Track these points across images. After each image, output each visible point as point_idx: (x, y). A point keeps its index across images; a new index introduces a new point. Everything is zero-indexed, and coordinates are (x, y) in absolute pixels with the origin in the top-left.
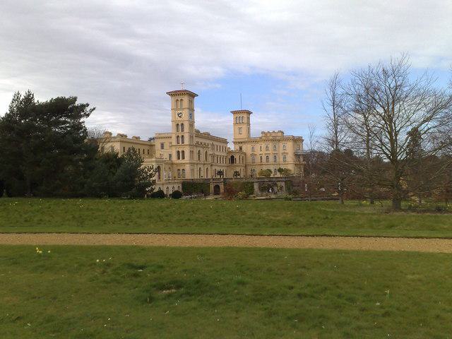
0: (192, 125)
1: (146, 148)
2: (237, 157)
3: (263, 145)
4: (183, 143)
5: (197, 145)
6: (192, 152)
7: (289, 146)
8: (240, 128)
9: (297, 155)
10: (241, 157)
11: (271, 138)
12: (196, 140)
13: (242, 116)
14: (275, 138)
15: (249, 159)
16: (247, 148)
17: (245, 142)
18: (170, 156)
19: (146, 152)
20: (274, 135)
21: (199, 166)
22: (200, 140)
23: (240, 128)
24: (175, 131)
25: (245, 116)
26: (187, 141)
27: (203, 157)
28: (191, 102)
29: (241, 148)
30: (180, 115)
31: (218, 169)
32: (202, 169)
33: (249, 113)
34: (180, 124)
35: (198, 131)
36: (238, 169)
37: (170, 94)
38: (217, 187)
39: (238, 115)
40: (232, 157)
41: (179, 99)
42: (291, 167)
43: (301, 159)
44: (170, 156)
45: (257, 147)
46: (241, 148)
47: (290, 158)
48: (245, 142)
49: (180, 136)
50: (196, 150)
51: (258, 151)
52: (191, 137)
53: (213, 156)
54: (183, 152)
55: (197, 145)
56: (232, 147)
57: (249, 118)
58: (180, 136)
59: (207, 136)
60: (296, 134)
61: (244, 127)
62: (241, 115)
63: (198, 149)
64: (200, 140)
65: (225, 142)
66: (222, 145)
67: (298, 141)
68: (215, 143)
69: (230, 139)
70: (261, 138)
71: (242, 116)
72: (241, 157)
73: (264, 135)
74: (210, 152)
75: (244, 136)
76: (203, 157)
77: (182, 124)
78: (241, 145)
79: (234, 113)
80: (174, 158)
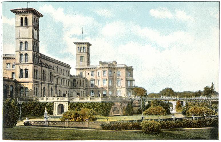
6: (35, 71)
13: (84, 48)
29: (81, 73)
33: (89, 45)
34: (24, 41)
37: (11, 10)
39: (80, 46)
40: (74, 80)
46: (81, 73)
56: (74, 72)
57: (88, 49)
58: (24, 53)
60: (129, 64)
61: (85, 56)
62: (83, 46)
65: (69, 67)
66: (66, 69)
68: (59, 66)
71: (84, 48)
77: (26, 42)
78: (82, 71)
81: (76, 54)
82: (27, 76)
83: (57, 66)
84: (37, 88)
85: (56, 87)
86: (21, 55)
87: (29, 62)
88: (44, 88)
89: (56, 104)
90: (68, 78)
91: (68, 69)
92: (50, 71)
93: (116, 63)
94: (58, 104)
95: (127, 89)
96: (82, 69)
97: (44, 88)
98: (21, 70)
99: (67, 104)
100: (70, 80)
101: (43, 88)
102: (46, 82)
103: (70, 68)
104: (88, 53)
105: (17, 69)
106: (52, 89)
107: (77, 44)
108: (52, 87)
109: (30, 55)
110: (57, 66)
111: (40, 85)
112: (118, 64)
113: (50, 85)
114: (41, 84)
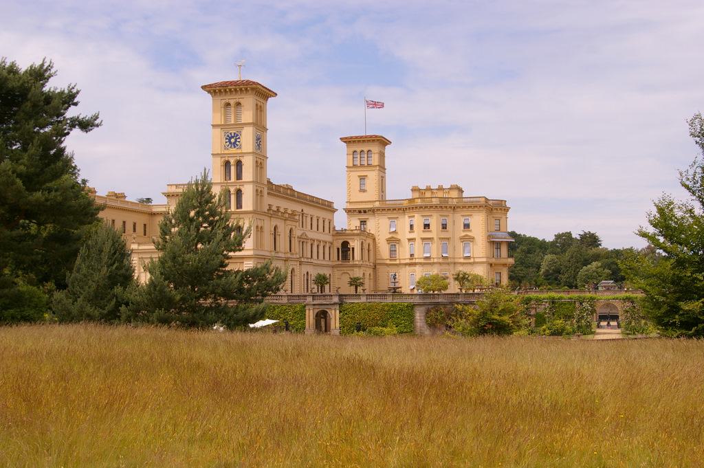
0: (260, 165)
1: (141, 220)
2: (355, 244)
3: (418, 220)
5: (272, 213)
6: (260, 229)
8: (362, 178)
9: (495, 244)
10: (366, 246)
11: (435, 202)
12: (268, 200)
14: (443, 204)
15: (384, 250)
16: (379, 227)
17: (373, 211)
19: (140, 229)
20: (440, 194)
23: (362, 178)
25: (375, 149)
27: (283, 244)
28: (260, 110)
29: (363, 222)
30: (233, 140)
31: (314, 272)
33: (383, 142)
34: (232, 161)
35: (269, 182)
36: (357, 273)
37: (204, 87)
38: (322, 316)
40: (345, 244)
41: (232, 102)
42: (480, 271)
43: (504, 250)
45: (404, 222)
46: (363, 222)
47: (480, 250)
48: (373, 211)
49: (232, 190)
50: (268, 225)
51: (404, 234)
52: (258, 194)
53: (303, 240)
55: (272, 213)
56: (341, 221)
57: (382, 155)
59: (286, 193)
60: (493, 195)
61: (373, 176)
63: (275, 222)
64: (276, 203)
65: (328, 207)
67: (496, 209)
68: (307, 210)
69: (340, 203)
70: (411, 200)
72: (366, 246)
73: (417, 195)
74: (298, 232)
75: (371, 194)
76: (283, 244)
78: (363, 217)
79: (348, 141)
81: (346, 169)
83: (302, 211)
87: (244, 209)
89: (311, 311)
92: (290, 227)
93: (461, 191)
94: (316, 311)
95: (491, 265)
96: (365, 212)
99: (338, 311)
100: (332, 243)
102: (280, 255)
103: (334, 211)
104: (382, 168)
107: (348, 141)
110: (302, 211)
112: (464, 195)
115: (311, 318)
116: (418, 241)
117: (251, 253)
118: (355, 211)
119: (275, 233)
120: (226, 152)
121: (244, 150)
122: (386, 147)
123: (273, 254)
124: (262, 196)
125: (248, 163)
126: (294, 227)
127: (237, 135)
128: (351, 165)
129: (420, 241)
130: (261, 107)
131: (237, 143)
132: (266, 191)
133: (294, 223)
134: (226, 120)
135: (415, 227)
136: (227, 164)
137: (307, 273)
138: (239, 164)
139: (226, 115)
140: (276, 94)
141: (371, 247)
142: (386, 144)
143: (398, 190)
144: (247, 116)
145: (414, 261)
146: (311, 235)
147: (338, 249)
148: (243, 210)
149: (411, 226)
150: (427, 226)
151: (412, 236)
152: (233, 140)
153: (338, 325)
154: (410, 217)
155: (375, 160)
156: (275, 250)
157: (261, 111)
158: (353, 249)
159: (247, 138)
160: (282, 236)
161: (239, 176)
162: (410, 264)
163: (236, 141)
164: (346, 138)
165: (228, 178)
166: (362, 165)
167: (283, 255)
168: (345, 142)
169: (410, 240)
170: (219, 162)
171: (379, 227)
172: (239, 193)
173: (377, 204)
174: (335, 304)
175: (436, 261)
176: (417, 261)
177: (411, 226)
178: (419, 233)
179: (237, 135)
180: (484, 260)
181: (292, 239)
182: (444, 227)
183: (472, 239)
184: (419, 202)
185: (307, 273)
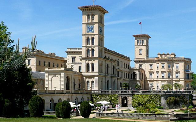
0: (101, 41)
2: (137, 73)
3: (160, 65)
4: (93, 55)
6: (100, 65)
7: (181, 66)
8: (140, 50)
16: (146, 67)
17: (144, 62)
18: (80, 67)
20: (168, 56)
21: (107, 79)
22: (108, 56)
23: (140, 50)
24: (84, 44)
26: (96, 55)
32: (110, 81)
34: (90, 37)
40: (134, 73)
44: (80, 67)
45: (155, 65)
46: (141, 65)
47: (181, 76)
49: (90, 49)
50: (105, 63)
52: (100, 51)
54: (93, 65)
61: (144, 49)
65: (128, 59)
66: (126, 62)
68: (121, 60)
69: (132, 59)
74: (116, 67)
80: (84, 70)
82: (93, 70)
84: (102, 81)
85: (118, 79)
86: (88, 50)
88: (108, 81)
89: (121, 97)
90: (128, 70)
91: (127, 62)
93: (175, 55)
95: (185, 81)
96: (141, 62)
97: (108, 81)
98: (88, 65)
99: (131, 97)
101: (107, 82)
102: (109, 75)
105: (84, 63)
106: (114, 82)
107: (136, 37)
108: (115, 80)
109: (96, 50)
111: (104, 78)
112: (176, 57)
113: (113, 78)
114: (106, 77)
115: (121, 100)
116: (160, 72)
117: (97, 74)
118: (138, 61)
119: (107, 66)
120: (88, 34)
121: (95, 33)
122: (149, 39)
123: (107, 75)
124: (102, 52)
125: (96, 38)
126: (115, 65)
127: (92, 27)
128: (137, 45)
129: (161, 72)
130: (102, 16)
131: (92, 30)
132: (104, 51)
133: (115, 64)
134: (88, 21)
135: (159, 68)
136: (88, 39)
137: (120, 83)
138: (93, 39)
139: (88, 19)
140: (108, 12)
141: (143, 75)
142: (149, 38)
143: (153, 55)
144: (96, 18)
145: (158, 79)
146: (121, 69)
147: (132, 75)
148: (94, 57)
149: (158, 67)
150: (163, 67)
151: (158, 70)
152: (90, 29)
153: (131, 103)
154: (157, 64)
155: (145, 43)
156: (107, 73)
157: (102, 18)
158: (137, 75)
159: (96, 28)
160: (110, 68)
161: (93, 43)
162: (157, 81)
163: (92, 30)
164: (135, 35)
165: (89, 44)
166: (140, 45)
167: (110, 75)
168: (135, 37)
169: (157, 72)
170: (84, 38)
171: (146, 67)
172: (93, 50)
173: (145, 59)
174: (130, 95)
175: (166, 79)
176: (160, 79)
177: (158, 67)
178: (160, 70)
179: (92, 27)
180: (183, 79)
181: (114, 70)
182: (169, 67)
183: (179, 72)
184: (160, 58)
185: (120, 83)
